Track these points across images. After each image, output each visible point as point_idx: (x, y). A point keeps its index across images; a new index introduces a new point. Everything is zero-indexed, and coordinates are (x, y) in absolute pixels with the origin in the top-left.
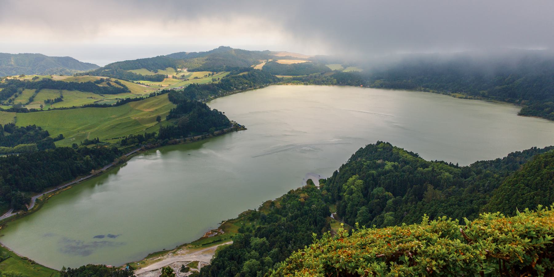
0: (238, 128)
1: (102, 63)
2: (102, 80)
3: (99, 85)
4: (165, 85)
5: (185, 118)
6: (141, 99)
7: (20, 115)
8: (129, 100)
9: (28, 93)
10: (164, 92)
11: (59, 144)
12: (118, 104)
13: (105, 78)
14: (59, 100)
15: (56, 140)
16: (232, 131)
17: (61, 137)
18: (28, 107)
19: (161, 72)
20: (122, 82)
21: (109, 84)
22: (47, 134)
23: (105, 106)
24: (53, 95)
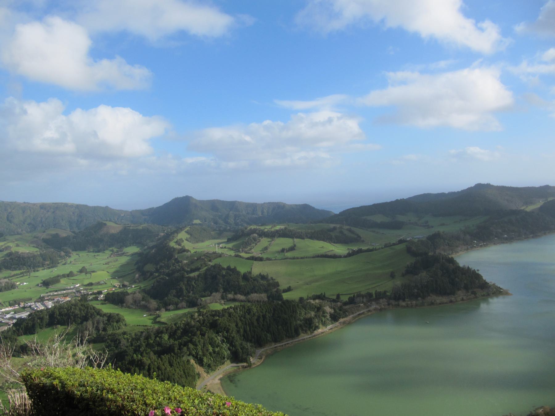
0: (498, 292)
1: (337, 211)
2: (335, 228)
4: (403, 234)
6: (376, 250)
8: (360, 251)
9: (264, 242)
10: (401, 242)
11: (285, 296)
12: (349, 255)
13: (338, 226)
15: (285, 291)
16: (488, 295)
17: (289, 290)
18: (264, 256)
19: (401, 218)
21: (341, 232)
22: (277, 285)
24: (287, 242)
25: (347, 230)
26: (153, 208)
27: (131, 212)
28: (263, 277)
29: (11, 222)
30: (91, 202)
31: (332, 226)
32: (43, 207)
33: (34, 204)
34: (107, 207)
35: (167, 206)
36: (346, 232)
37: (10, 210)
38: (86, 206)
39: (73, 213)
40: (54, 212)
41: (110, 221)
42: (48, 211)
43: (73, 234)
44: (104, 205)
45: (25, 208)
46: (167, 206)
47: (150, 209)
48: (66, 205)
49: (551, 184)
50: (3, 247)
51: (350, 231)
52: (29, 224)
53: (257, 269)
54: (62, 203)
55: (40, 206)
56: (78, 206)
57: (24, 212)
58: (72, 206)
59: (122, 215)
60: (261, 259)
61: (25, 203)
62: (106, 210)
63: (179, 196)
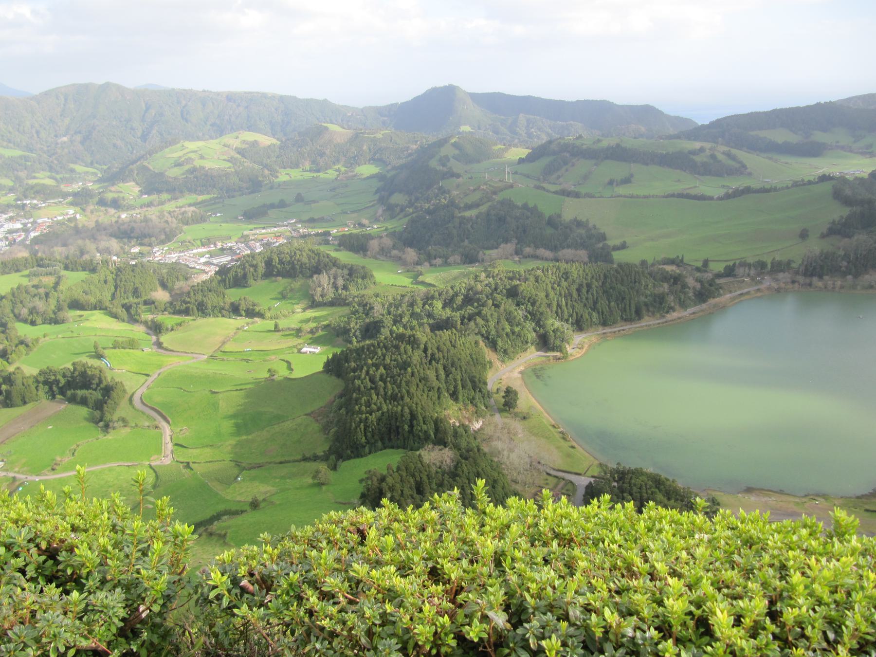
1: (703, 118)
2: (702, 150)
3: (698, 159)
5: (861, 239)
6: (775, 189)
7: (567, 199)
8: (748, 190)
9: (582, 166)
10: (824, 178)
12: (728, 196)
13: (707, 145)
14: (627, 181)
18: (583, 190)
19: (819, 137)
20: (743, 155)
21: (713, 157)
23: (702, 198)
25: (724, 153)
26: (396, 104)
27: (362, 110)
28: (579, 224)
29: (187, 121)
30: (303, 93)
31: (697, 145)
32: (230, 98)
33: (218, 94)
34: (325, 101)
35: (418, 102)
36: (720, 157)
37: (184, 103)
38: (295, 98)
39: (276, 109)
40: (247, 107)
41: (332, 123)
42: (239, 106)
43: (279, 143)
44: (320, 97)
45: (205, 99)
46: (417, 101)
47: (392, 105)
48: (264, 96)
49: (874, 92)
50: (183, 159)
51: (729, 155)
52: (213, 125)
53: (570, 210)
54: (258, 93)
55: (227, 97)
56: (282, 99)
57: (204, 105)
58: (273, 97)
59: (349, 114)
60: (577, 195)
61: (204, 91)
62: (324, 105)
63: (438, 86)
